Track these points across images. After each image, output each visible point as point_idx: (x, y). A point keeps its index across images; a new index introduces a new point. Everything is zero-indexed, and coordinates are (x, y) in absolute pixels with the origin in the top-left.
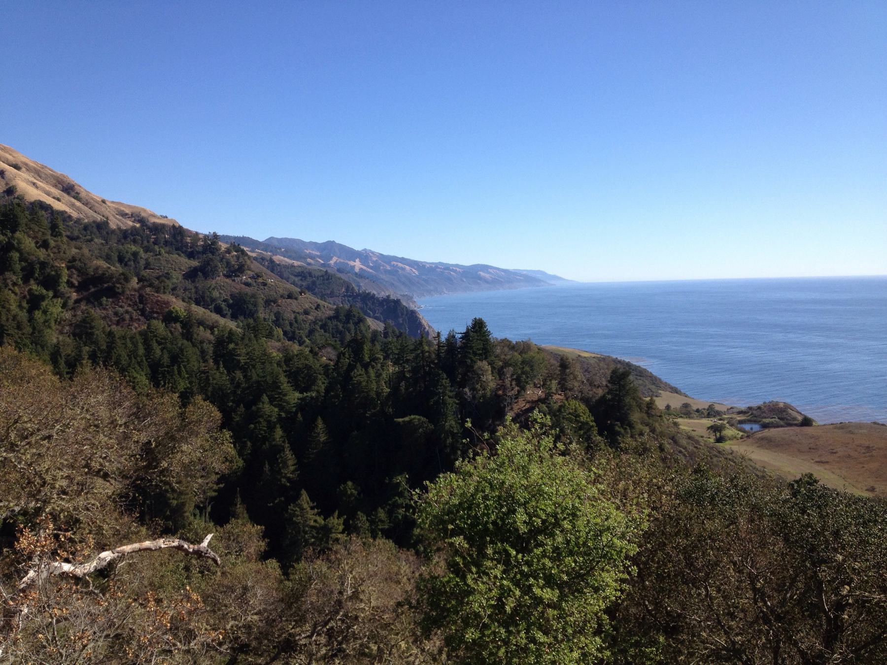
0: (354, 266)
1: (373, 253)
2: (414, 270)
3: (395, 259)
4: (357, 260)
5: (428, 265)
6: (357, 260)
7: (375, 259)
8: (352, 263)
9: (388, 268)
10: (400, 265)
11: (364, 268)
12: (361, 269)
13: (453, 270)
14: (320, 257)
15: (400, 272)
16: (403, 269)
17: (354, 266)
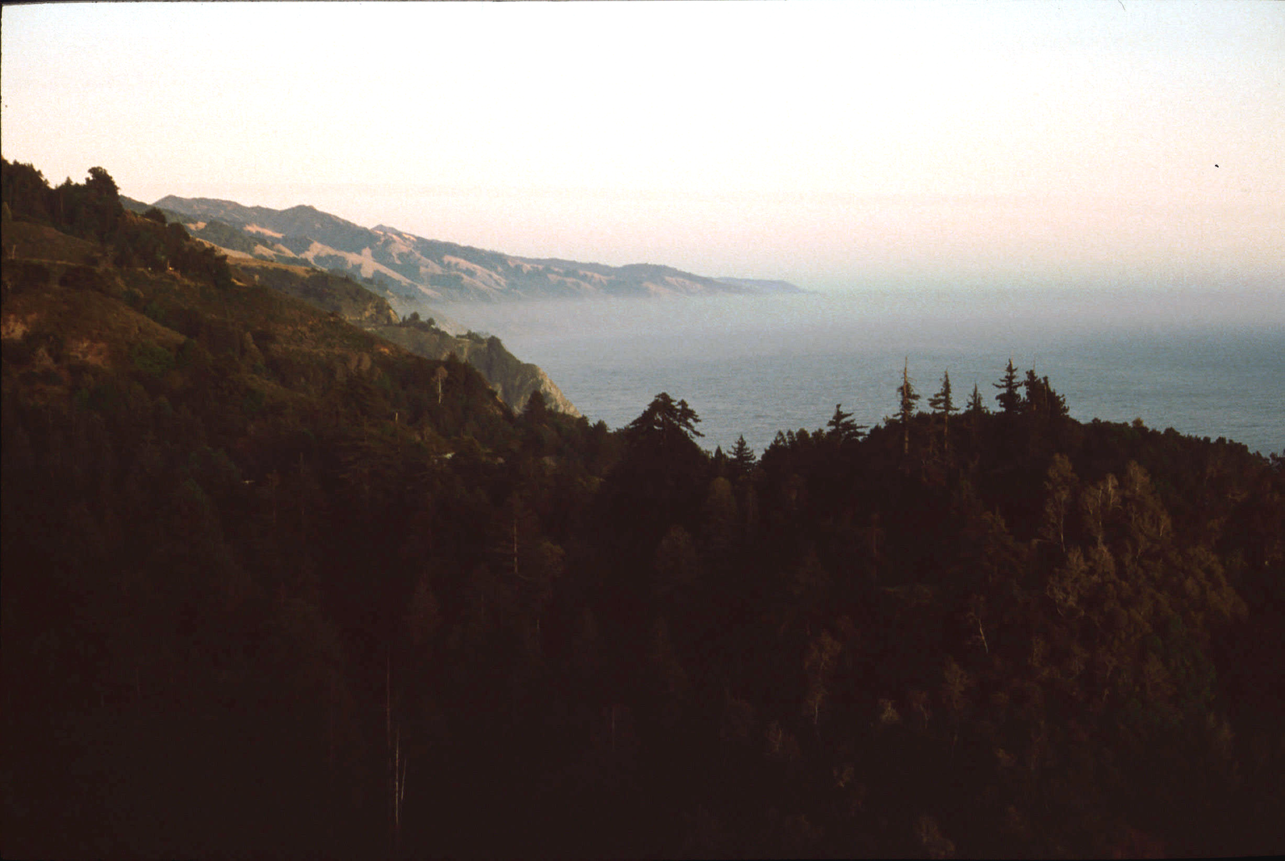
0: (359, 267)
1: (399, 234)
2: (495, 276)
3: (451, 249)
4: (367, 252)
5: (527, 267)
6: (367, 252)
7: (405, 249)
8: (352, 258)
9: (438, 270)
10: (464, 263)
11: (384, 270)
12: (377, 272)
13: (584, 278)
14: (285, 241)
15: (466, 278)
16: (471, 273)
17: (359, 267)
